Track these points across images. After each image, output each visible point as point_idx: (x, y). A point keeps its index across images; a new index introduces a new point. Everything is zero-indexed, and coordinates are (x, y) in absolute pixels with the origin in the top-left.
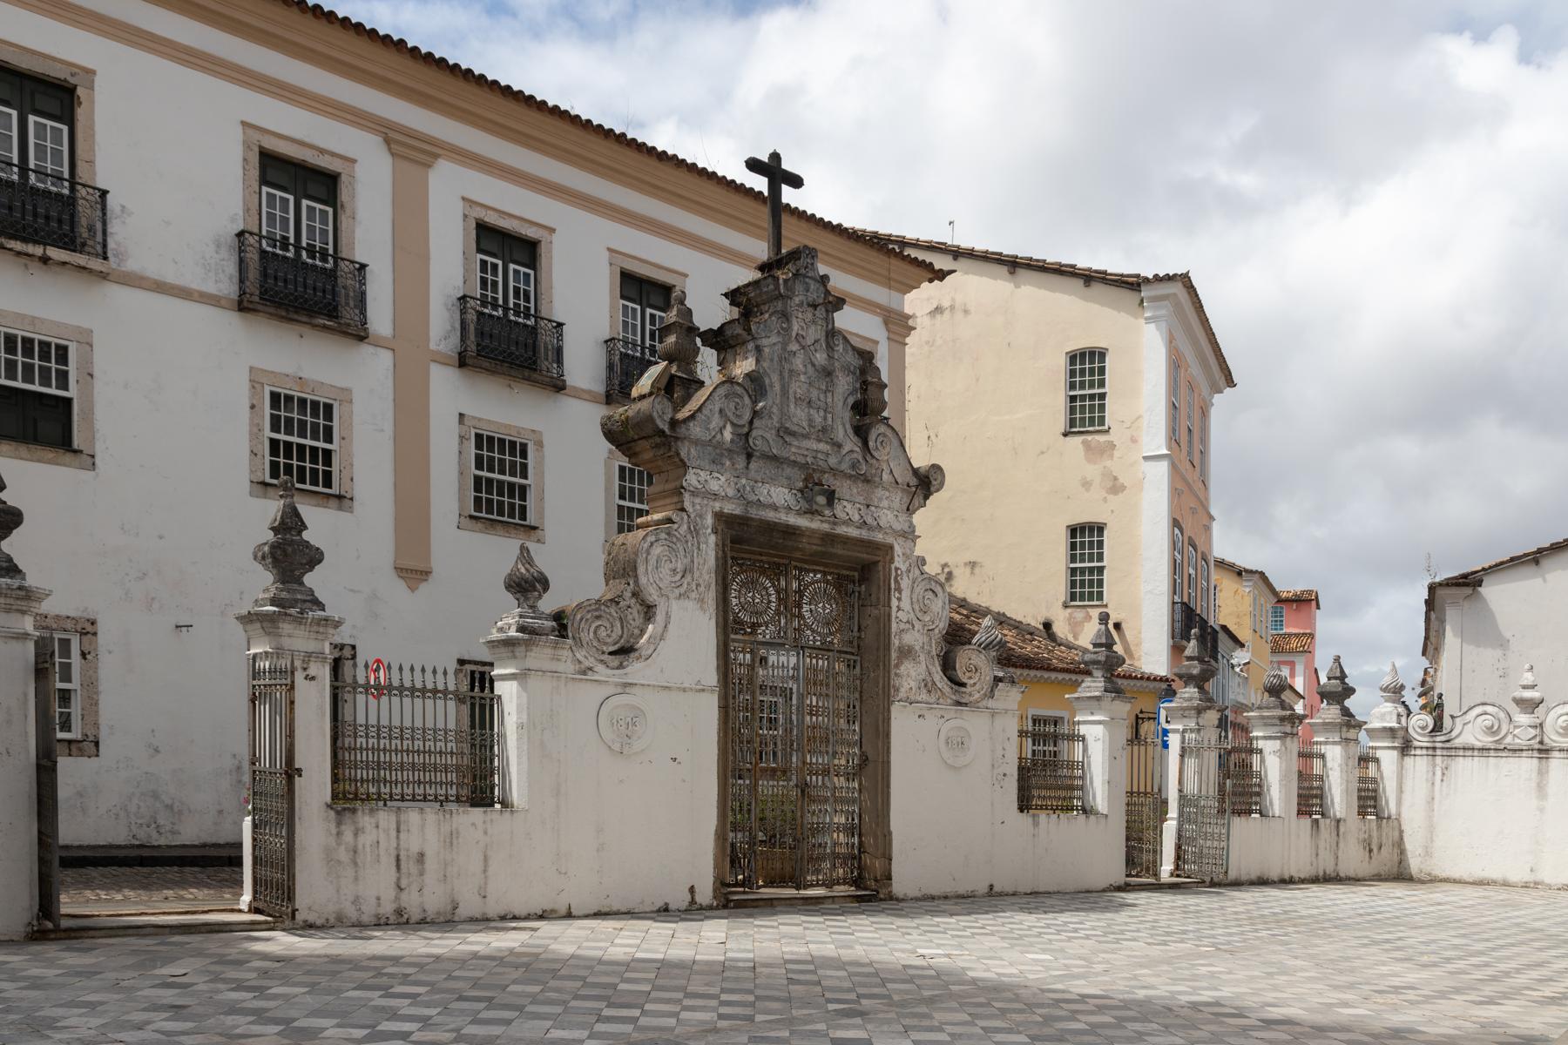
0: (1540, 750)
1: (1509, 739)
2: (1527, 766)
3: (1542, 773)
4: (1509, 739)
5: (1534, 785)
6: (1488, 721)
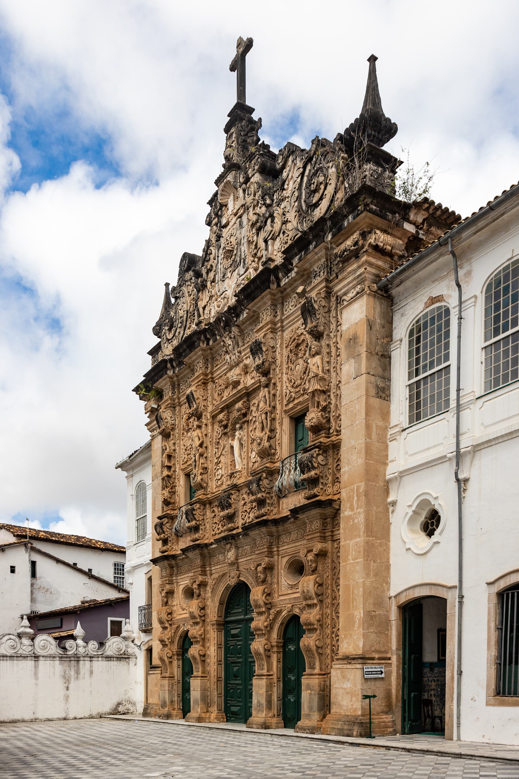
0: (35, 657)
1: (21, 651)
2: (30, 663)
3: (36, 667)
4: (19, 652)
5: (33, 673)
6: (12, 643)
